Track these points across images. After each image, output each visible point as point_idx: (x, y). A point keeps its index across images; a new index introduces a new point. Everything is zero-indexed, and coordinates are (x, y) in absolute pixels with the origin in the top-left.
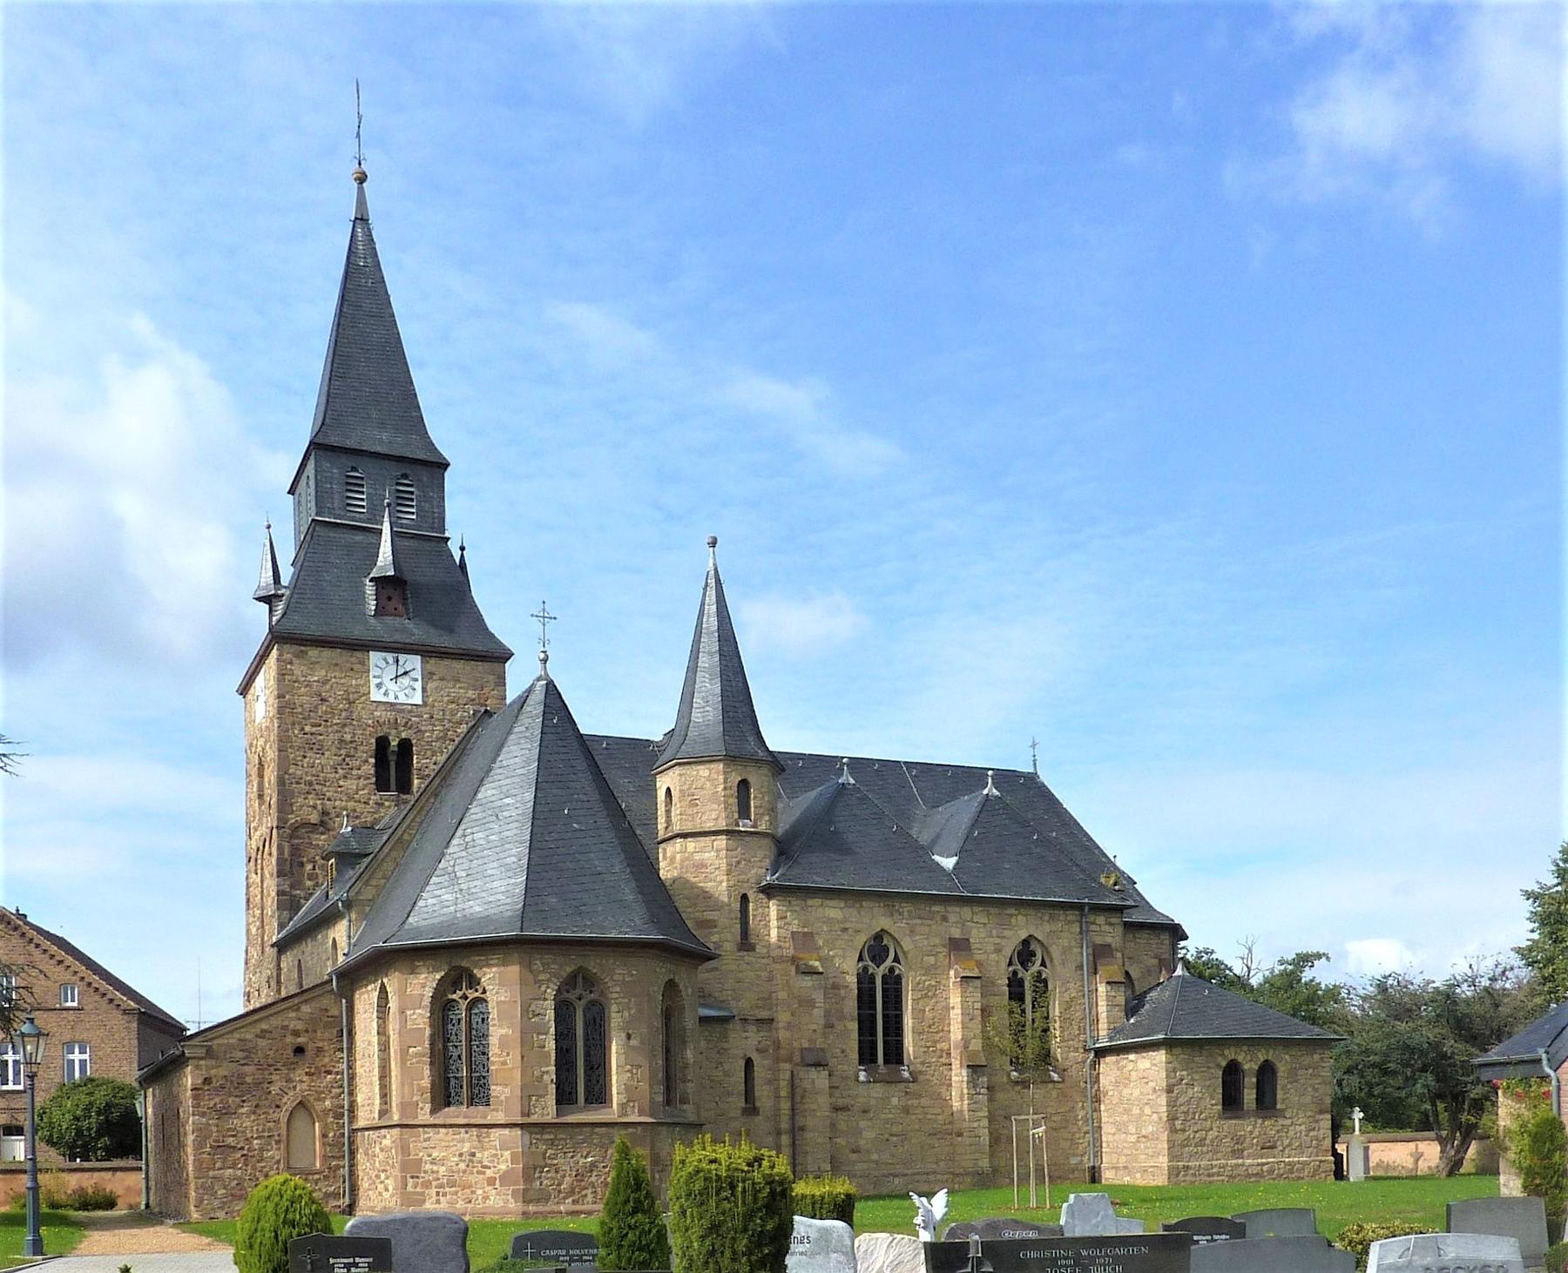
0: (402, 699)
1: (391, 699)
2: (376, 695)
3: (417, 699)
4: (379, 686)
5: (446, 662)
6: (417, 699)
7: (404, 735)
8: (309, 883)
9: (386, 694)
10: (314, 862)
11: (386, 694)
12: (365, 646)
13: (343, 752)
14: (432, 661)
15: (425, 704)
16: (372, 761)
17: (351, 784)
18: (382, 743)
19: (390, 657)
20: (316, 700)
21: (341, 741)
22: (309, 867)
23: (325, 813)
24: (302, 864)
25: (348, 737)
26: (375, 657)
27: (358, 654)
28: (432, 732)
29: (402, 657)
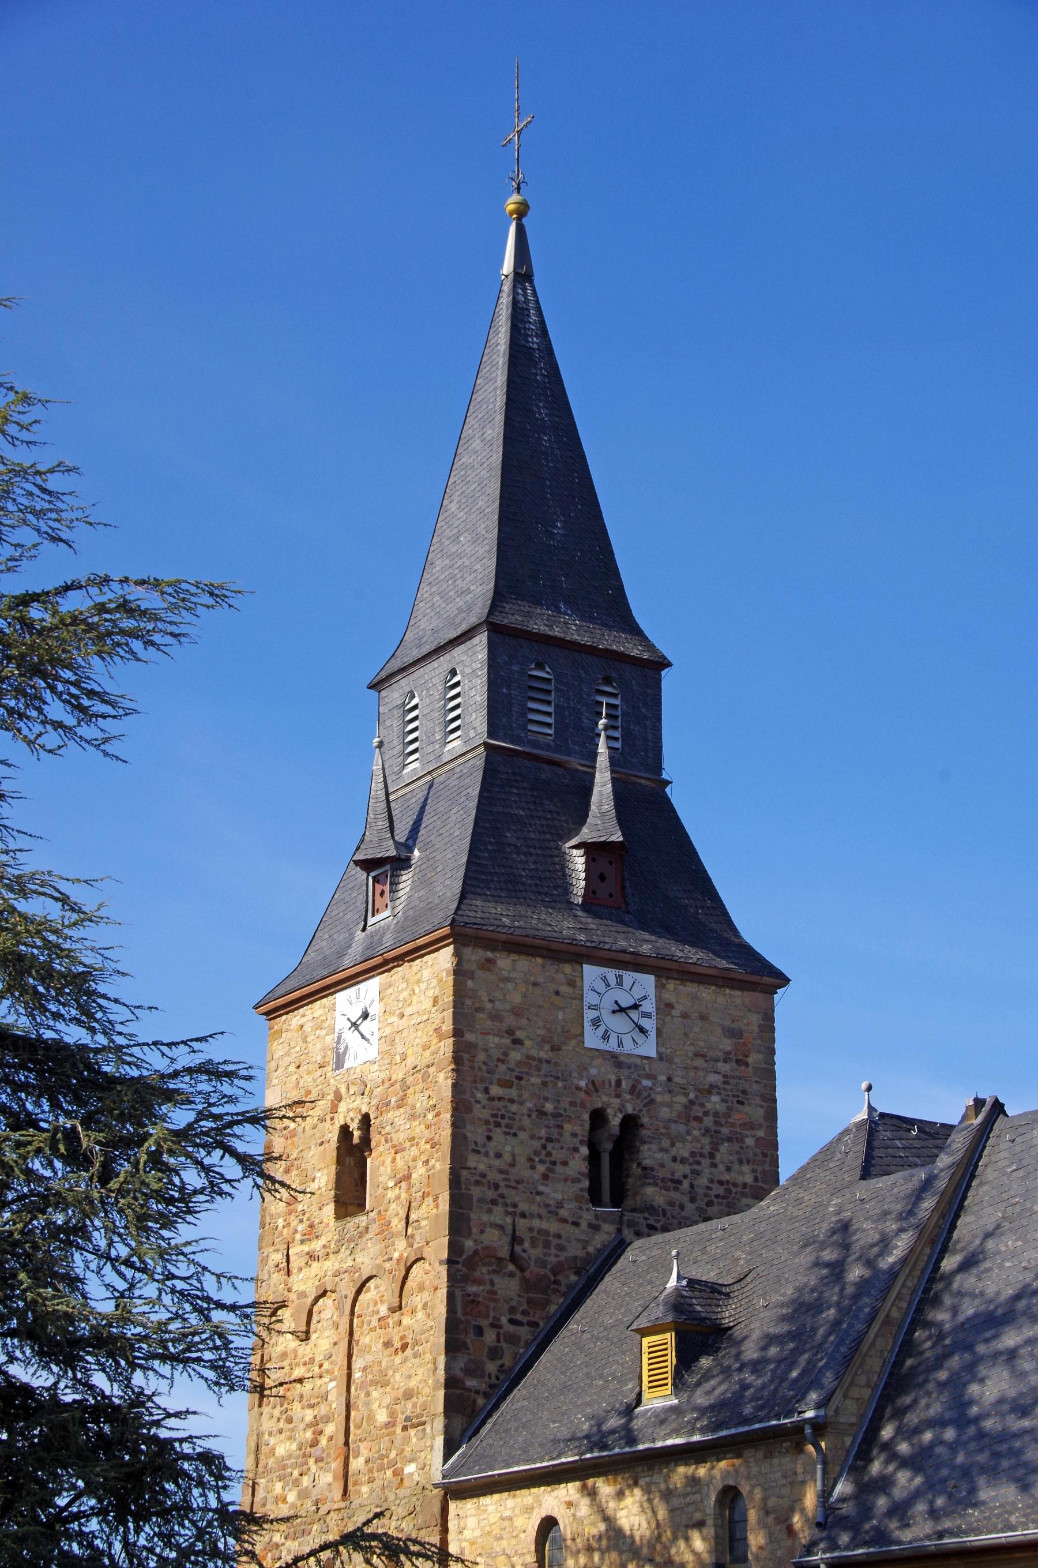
0: (628, 1046)
1: (612, 1045)
2: (592, 1039)
3: (649, 1048)
4: (596, 1022)
5: (691, 988)
6: (649, 1048)
7: (629, 1109)
8: (491, 1367)
9: (606, 1037)
10: (495, 1325)
11: (606, 1037)
12: (578, 955)
13: (543, 1133)
14: (671, 985)
15: (661, 1057)
16: (585, 1151)
17: (554, 1192)
18: (598, 1117)
19: (611, 974)
20: (507, 1041)
21: (542, 1113)
22: (490, 1337)
23: (515, 1239)
24: (479, 1331)
25: (549, 1107)
26: (591, 972)
27: (567, 968)
28: (668, 1108)
29: (628, 977)
